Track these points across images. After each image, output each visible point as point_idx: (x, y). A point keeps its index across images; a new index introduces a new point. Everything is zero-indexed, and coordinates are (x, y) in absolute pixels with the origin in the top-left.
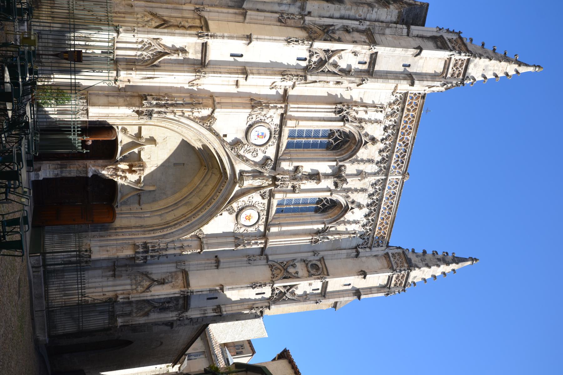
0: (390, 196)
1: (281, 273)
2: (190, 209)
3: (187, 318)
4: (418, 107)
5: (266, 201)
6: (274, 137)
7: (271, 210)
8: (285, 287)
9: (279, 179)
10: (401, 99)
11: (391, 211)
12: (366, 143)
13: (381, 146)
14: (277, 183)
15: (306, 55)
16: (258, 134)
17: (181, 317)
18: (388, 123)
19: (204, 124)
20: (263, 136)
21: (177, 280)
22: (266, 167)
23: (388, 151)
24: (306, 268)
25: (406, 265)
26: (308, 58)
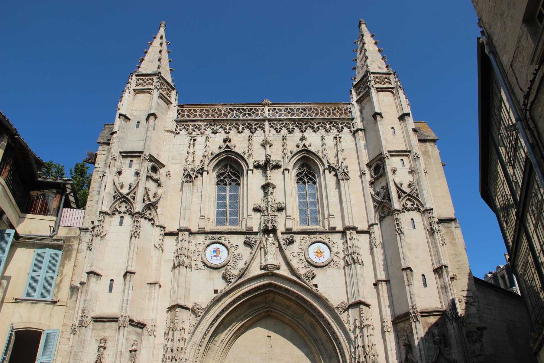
0: (289, 112)
1: (386, 206)
2: (316, 324)
3: (453, 309)
4: (192, 109)
5: (297, 238)
6: (218, 239)
7: (309, 231)
8: (399, 197)
9: (266, 226)
10: (183, 125)
11: (307, 108)
12: (227, 147)
13: (233, 131)
14: (270, 228)
15: (117, 217)
16: (215, 256)
17: (453, 317)
18: (209, 131)
19: (199, 316)
20: (216, 251)
21: (405, 328)
22: (253, 242)
23: (239, 125)
24: (379, 180)
25: (365, 79)
26: (122, 214)
